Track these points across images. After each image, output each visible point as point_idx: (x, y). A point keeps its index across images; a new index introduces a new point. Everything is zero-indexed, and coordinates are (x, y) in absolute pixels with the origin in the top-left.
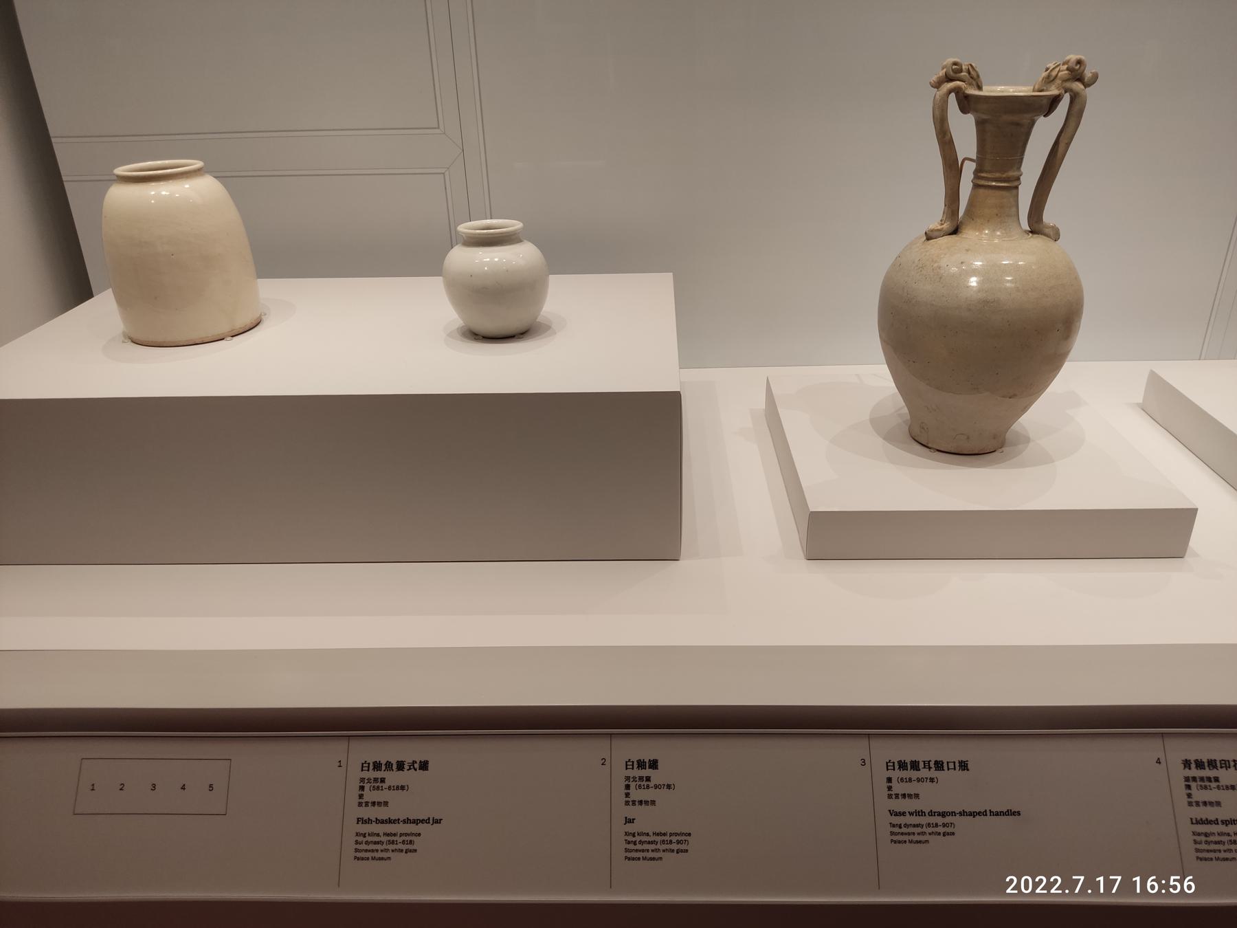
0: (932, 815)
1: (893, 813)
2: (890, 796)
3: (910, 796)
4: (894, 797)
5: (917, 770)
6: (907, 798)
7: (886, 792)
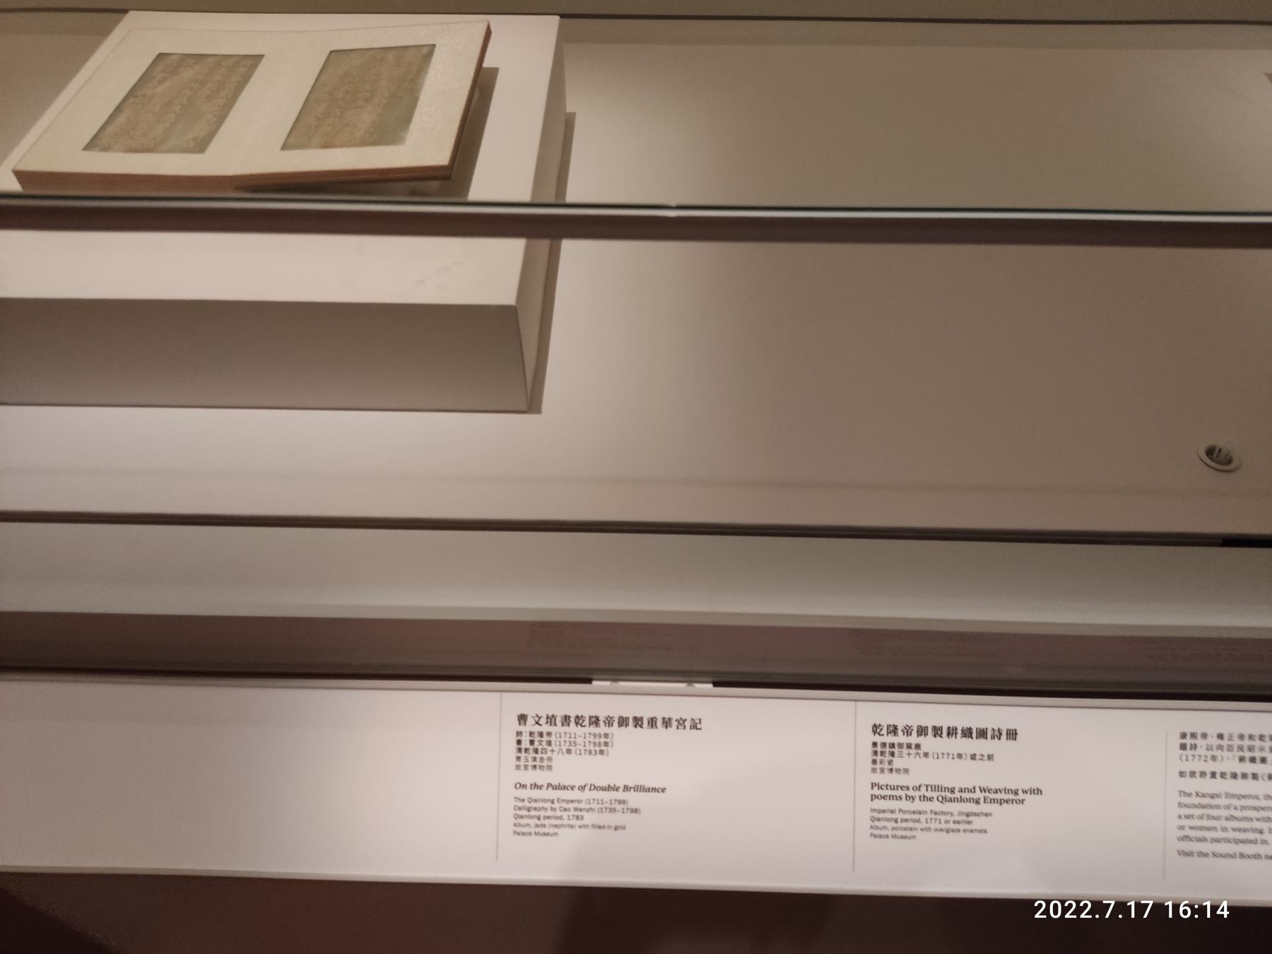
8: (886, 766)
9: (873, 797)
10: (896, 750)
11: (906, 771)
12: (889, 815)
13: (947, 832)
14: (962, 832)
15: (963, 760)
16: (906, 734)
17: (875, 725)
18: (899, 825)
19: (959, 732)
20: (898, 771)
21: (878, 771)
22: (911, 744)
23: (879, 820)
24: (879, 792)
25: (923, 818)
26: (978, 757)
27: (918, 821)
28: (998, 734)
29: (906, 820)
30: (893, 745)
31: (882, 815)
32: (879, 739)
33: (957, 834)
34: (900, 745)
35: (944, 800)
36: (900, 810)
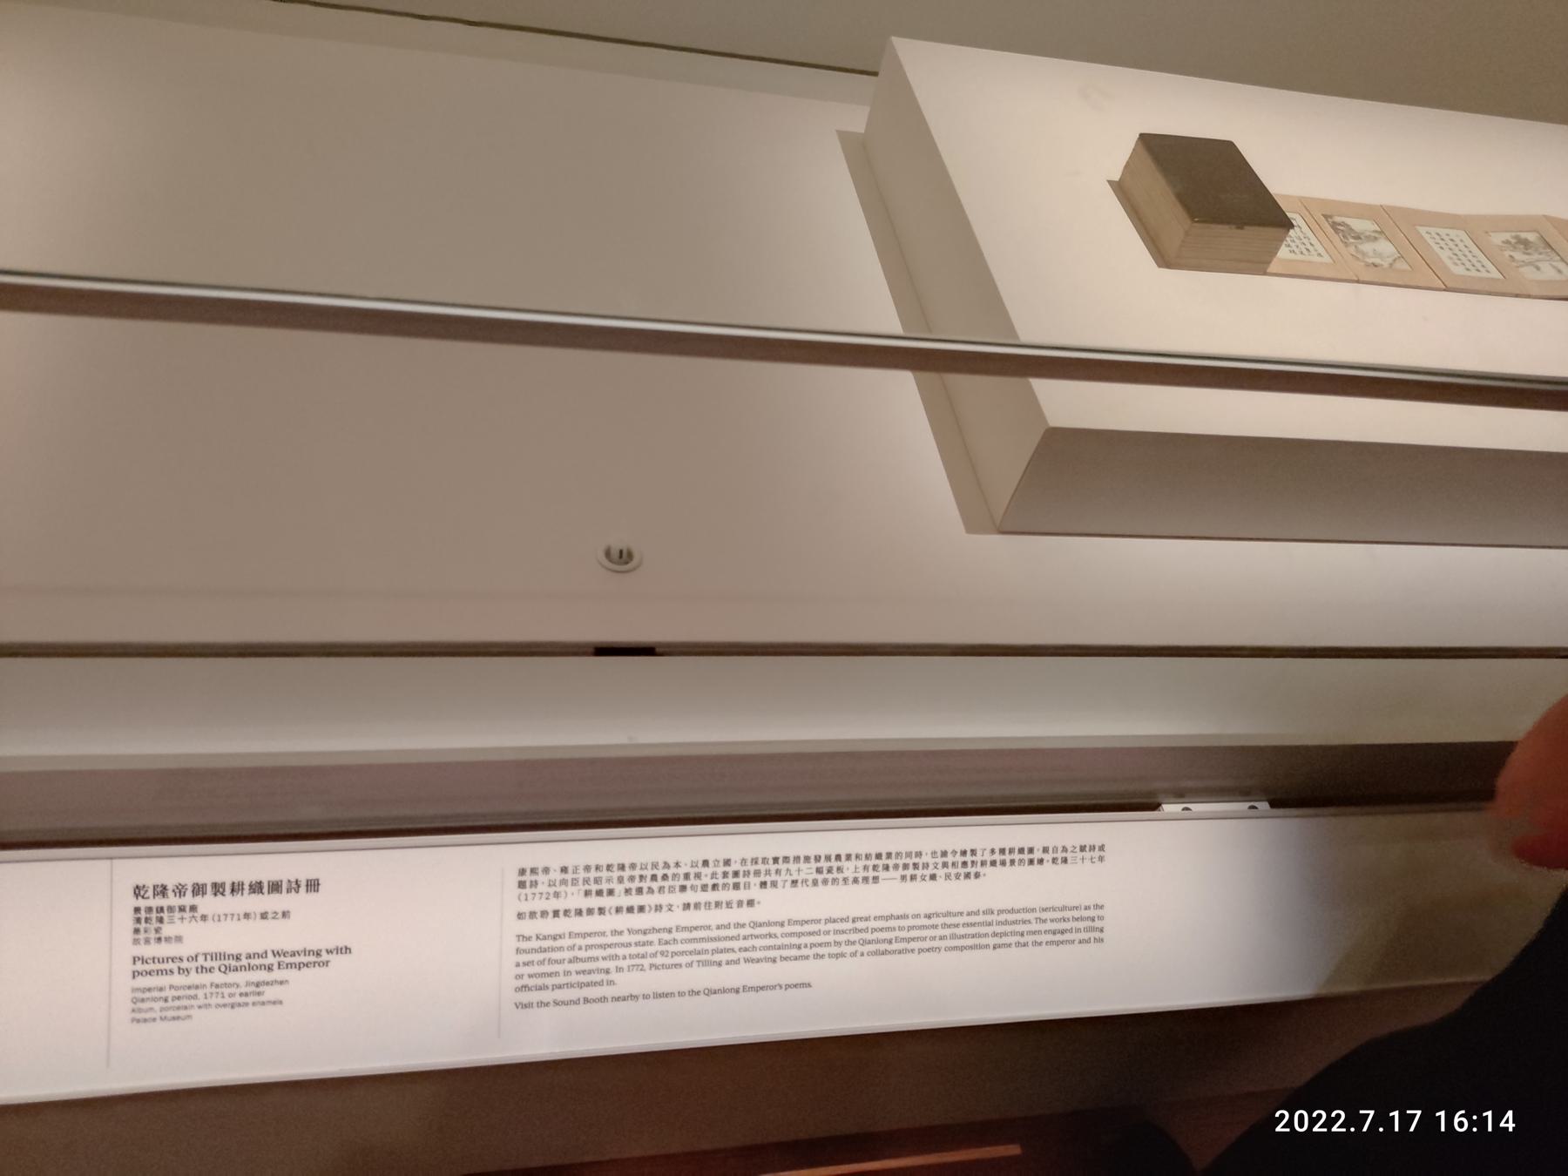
8: (153, 935)
9: (135, 974)
10: (165, 915)
11: (179, 939)
12: (156, 994)
13: (232, 1007)
14: (251, 1006)
15: (251, 921)
16: (178, 894)
17: (137, 887)
18: (170, 1004)
19: (246, 887)
20: (168, 939)
21: (142, 942)
23: (143, 1000)
24: (142, 966)
25: (200, 993)
26: (270, 916)
27: (195, 997)
28: (295, 886)
29: (179, 998)
30: (162, 909)
31: (148, 995)
32: (142, 903)
34: (171, 909)
35: (228, 969)
36: (171, 987)
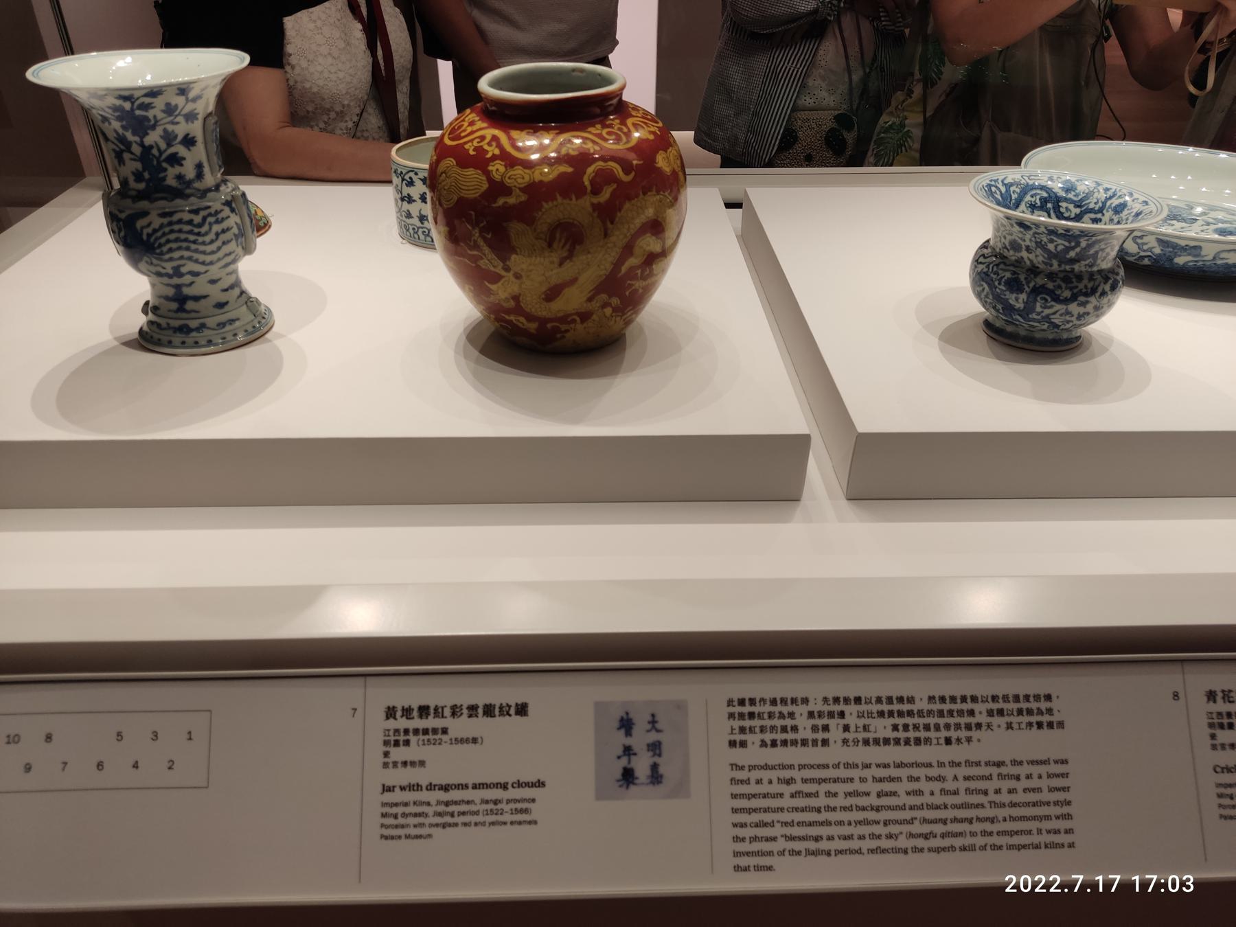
0: (431, 789)
1: (387, 789)
2: (386, 765)
3: (413, 764)
4: (391, 765)
5: (491, 717)
6: (409, 767)
7: (382, 759)
14: (509, 824)
22: (427, 729)
33: (503, 827)
